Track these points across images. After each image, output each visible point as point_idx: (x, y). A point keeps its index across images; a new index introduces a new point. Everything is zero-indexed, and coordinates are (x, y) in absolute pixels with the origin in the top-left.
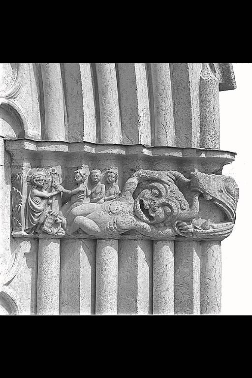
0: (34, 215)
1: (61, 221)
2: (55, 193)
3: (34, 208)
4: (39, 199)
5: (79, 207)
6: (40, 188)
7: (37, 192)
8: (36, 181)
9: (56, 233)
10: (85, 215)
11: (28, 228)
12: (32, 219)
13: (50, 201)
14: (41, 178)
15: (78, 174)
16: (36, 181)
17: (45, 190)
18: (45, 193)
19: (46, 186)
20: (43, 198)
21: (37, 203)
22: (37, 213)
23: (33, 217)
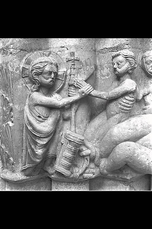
0: (36, 144)
1: (88, 152)
2: (77, 97)
3: (34, 129)
4: (42, 111)
5: (124, 124)
6: (49, 89)
7: (40, 97)
8: (38, 74)
9: (81, 175)
10: (135, 139)
11: (27, 166)
12: (32, 150)
13: (67, 115)
14: (47, 69)
15: (120, 58)
16: (38, 74)
17: (59, 92)
18: (57, 99)
19: (59, 85)
20: (51, 108)
21: (42, 119)
22: (40, 138)
23: (33, 146)
